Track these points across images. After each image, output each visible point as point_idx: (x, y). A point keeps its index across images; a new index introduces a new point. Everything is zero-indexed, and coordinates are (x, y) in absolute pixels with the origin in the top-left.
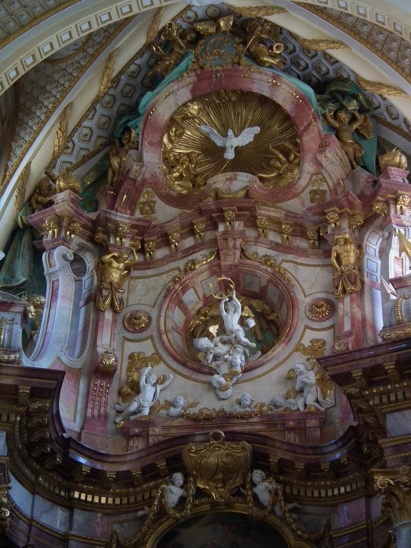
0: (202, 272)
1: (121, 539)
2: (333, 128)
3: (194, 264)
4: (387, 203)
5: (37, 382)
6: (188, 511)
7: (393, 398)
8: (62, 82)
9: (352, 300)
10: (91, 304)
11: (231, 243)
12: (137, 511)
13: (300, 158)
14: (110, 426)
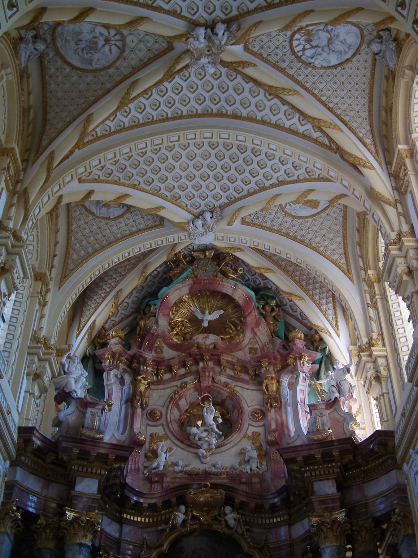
0: (190, 389)
1: (149, 543)
2: (261, 314)
4: (295, 359)
5: (119, 452)
6: (188, 529)
7: (318, 473)
8: (114, 276)
9: (275, 411)
10: (129, 403)
11: (207, 374)
12: (157, 526)
13: (243, 329)
14: (141, 475)
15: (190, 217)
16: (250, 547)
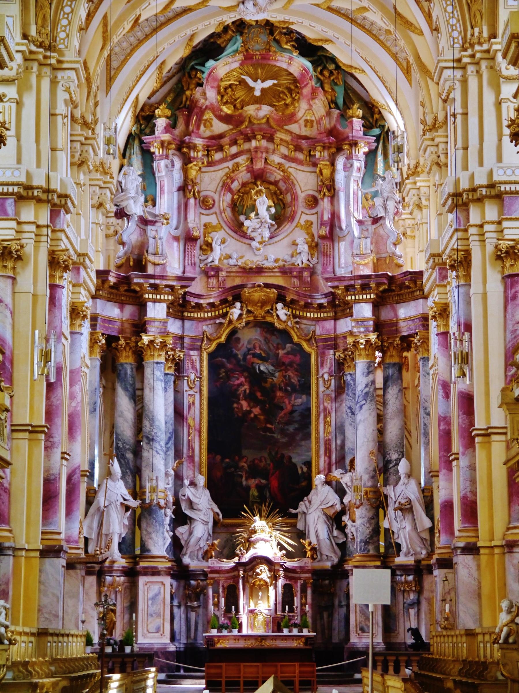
0: (242, 172)
2: (318, 79)
3: (238, 167)
4: (351, 145)
10: (181, 192)
14: (198, 269)
16: (299, 338)
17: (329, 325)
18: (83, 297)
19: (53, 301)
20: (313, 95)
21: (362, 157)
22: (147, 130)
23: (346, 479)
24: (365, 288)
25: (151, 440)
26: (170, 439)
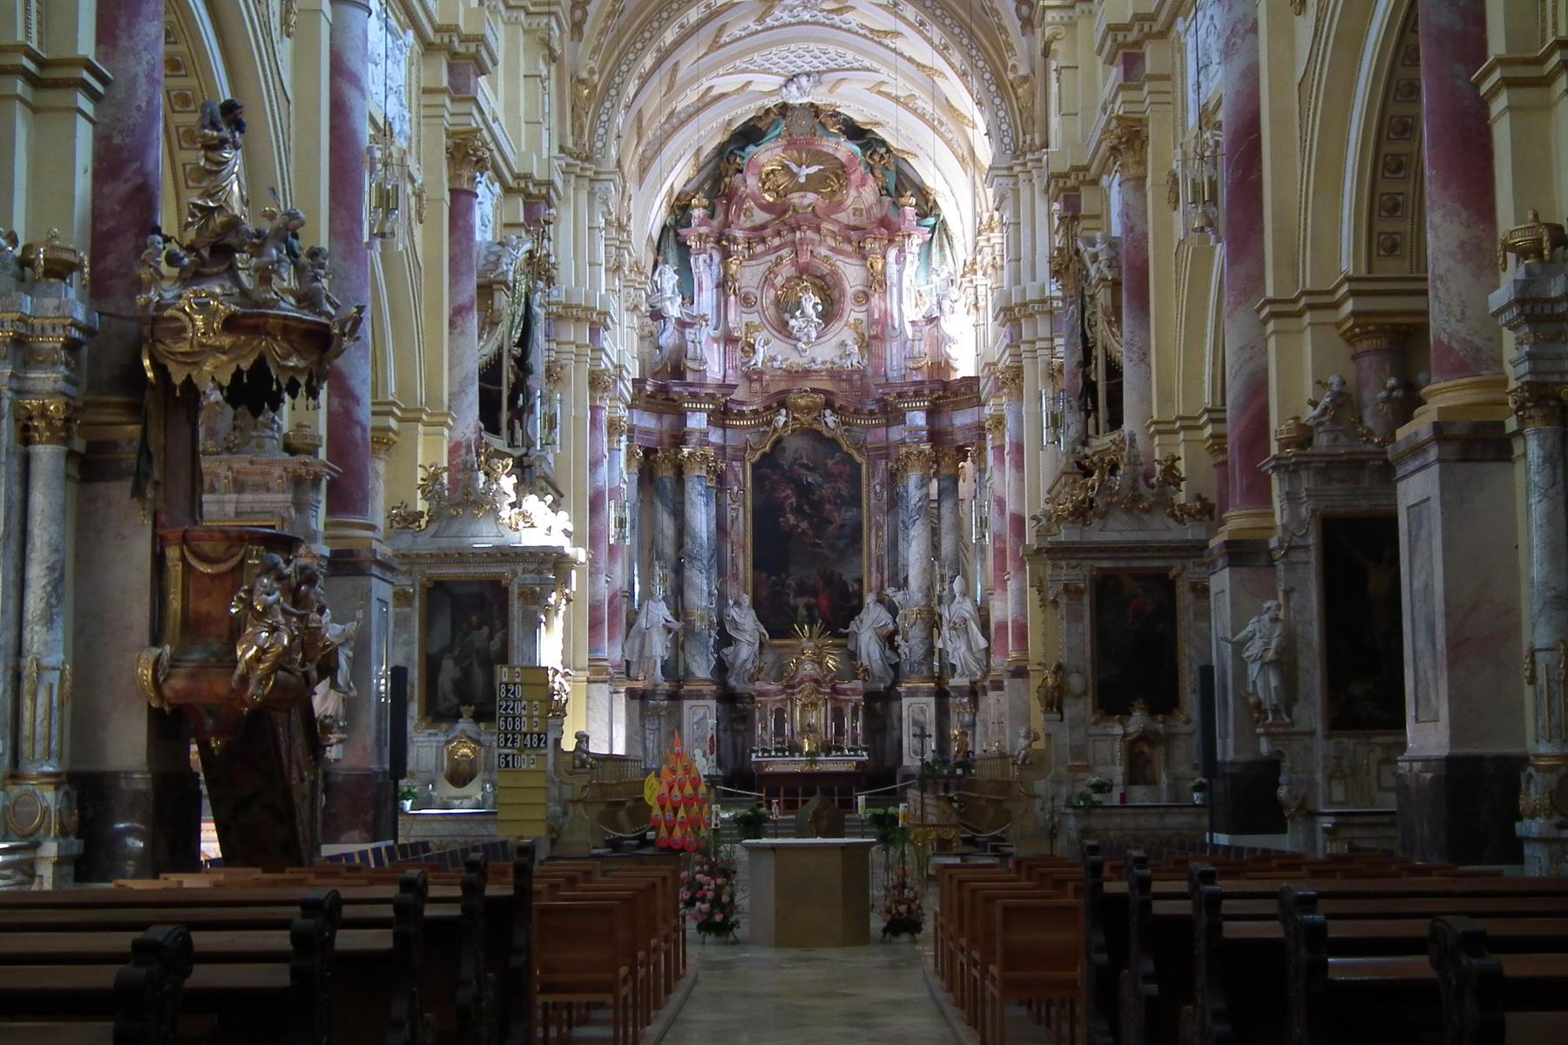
14: (739, 372)
15: (781, 80)
17: (881, 432)
18: (623, 413)
19: (594, 423)
20: (863, 183)
21: (916, 249)
22: (683, 222)
23: (898, 597)
24: (917, 394)
25: (692, 559)
26: (712, 556)
